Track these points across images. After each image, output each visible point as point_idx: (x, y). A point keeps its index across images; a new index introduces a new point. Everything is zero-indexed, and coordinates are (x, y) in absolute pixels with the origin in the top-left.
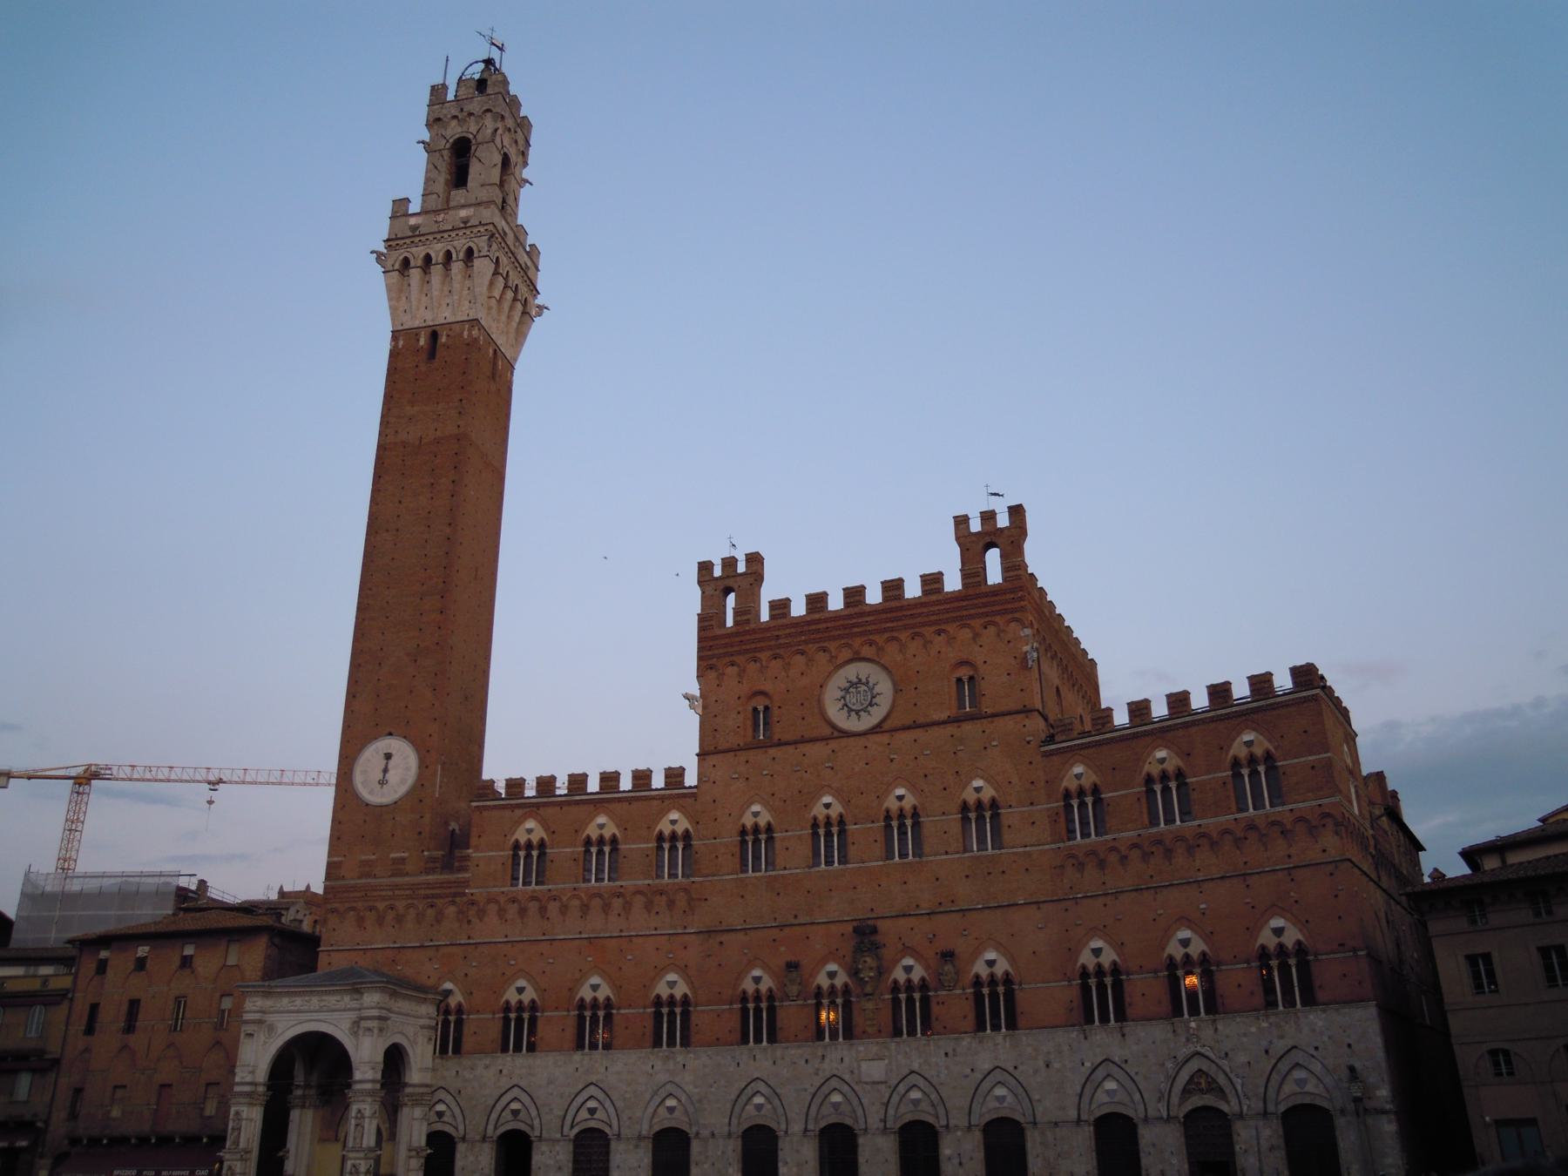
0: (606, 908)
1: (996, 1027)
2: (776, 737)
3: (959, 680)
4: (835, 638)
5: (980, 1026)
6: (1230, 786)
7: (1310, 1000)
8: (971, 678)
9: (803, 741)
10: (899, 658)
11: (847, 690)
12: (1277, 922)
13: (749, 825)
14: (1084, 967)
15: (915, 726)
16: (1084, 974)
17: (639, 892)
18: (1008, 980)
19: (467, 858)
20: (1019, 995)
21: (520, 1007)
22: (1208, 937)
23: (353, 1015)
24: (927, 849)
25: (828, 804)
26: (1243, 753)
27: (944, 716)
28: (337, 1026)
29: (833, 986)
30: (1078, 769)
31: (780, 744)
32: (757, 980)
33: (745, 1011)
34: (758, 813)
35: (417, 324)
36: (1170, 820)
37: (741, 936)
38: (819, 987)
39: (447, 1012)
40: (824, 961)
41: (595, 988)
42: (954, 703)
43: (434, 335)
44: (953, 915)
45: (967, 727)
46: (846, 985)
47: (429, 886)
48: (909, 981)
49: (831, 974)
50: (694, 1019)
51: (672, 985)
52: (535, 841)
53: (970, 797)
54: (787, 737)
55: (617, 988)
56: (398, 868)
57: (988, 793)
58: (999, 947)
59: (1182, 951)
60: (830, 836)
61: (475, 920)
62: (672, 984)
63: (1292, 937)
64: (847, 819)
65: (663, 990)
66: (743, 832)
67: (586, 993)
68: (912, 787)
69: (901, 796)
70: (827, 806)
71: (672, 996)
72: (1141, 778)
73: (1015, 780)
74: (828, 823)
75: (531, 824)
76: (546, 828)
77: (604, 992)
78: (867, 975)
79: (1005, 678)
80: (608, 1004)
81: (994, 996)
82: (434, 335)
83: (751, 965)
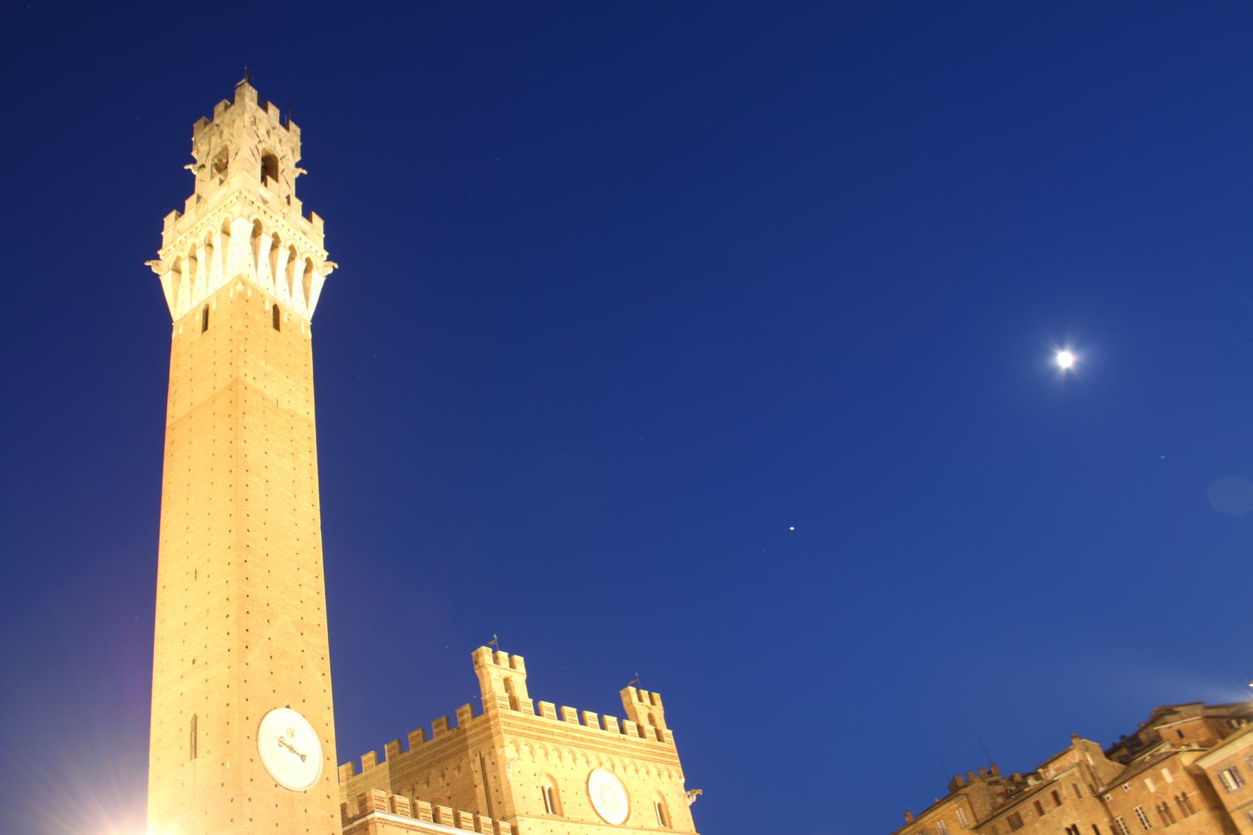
2: (566, 815)
9: (582, 821)
54: (573, 817)
82: (276, 309)
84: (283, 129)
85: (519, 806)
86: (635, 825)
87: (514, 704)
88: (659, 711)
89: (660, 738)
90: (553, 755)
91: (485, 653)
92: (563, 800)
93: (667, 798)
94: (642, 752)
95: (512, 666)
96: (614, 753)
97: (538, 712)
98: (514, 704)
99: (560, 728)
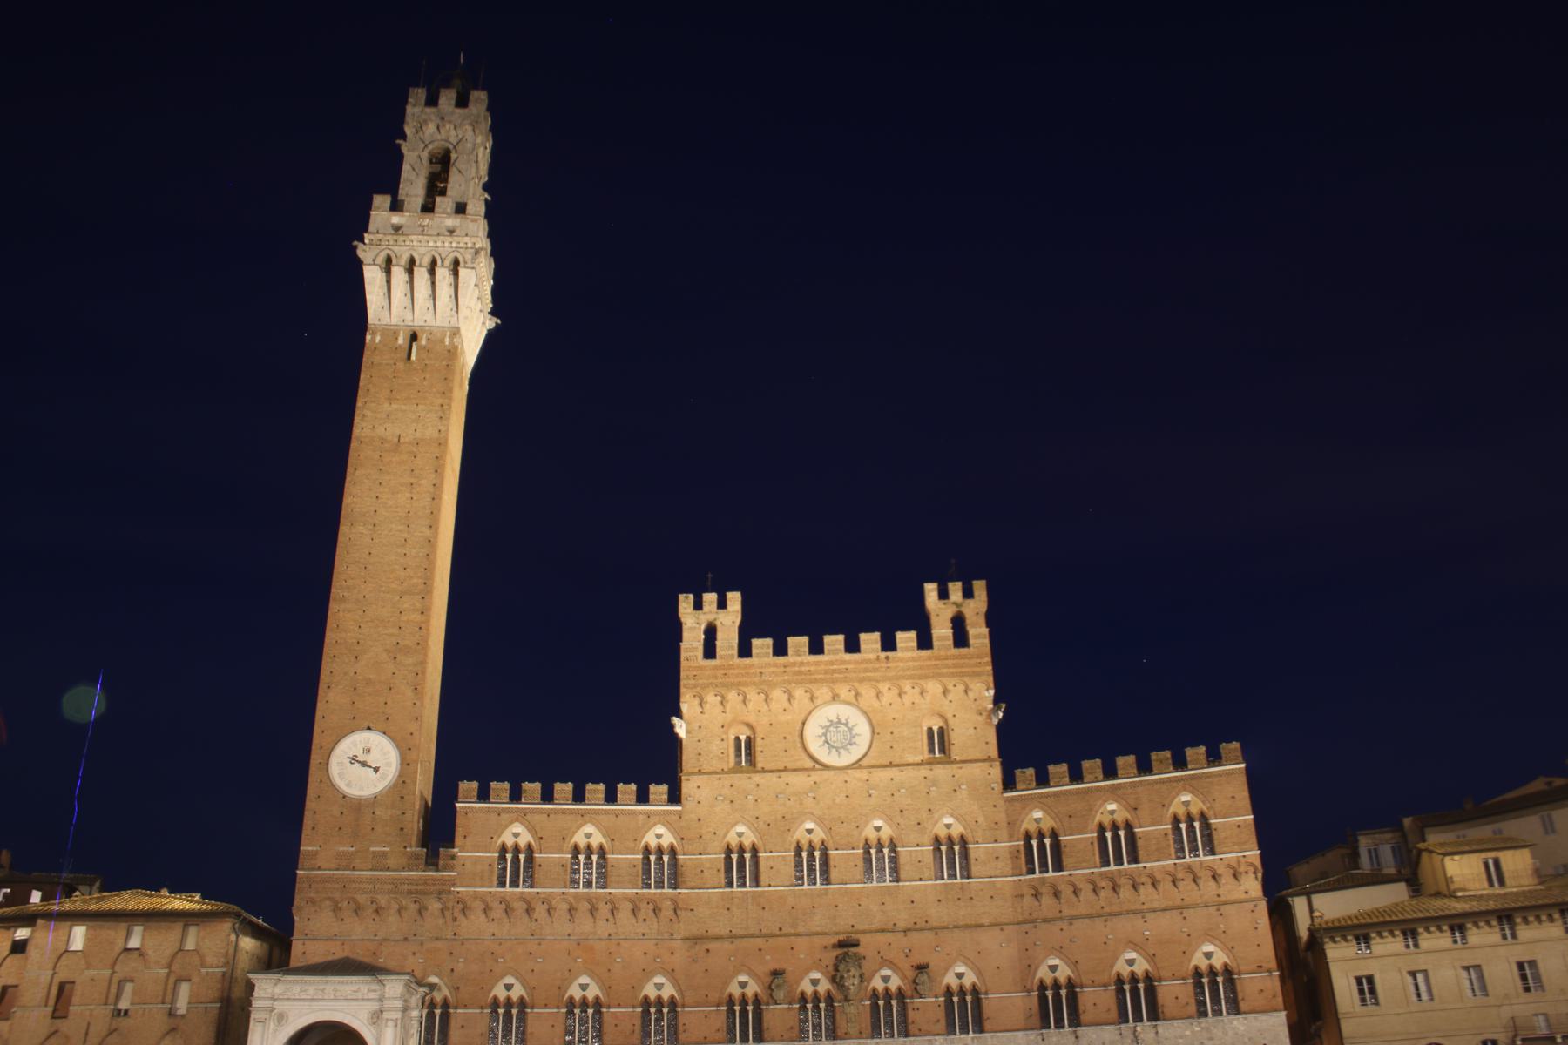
0: (593, 911)
1: (965, 1030)
2: (759, 766)
3: (930, 730)
4: (816, 681)
5: (951, 1029)
6: (1171, 837)
7: (1235, 1008)
8: (941, 731)
9: (785, 770)
10: (876, 704)
11: (827, 728)
12: (1209, 948)
13: (734, 844)
14: (1041, 981)
15: (891, 765)
16: (1042, 987)
17: (626, 898)
18: (975, 991)
19: (453, 857)
20: (985, 1003)
21: (509, 1004)
22: (1151, 958)
23: (375, 1006)
24: (903, 875)
25: (809, 830)
26: (1181, 812)
27: (918, 759)
28: (355, 1017)
29: (816, 993)
30: (1038, 814)
31: (763, 771)
32: (743, 985)
33: (731, 1011)
34: (742, 833)
35: (394, 321)
36: (1119, 861)
37: (726, 945)
38: (803, 993)
39: (432, 1005)
40: (808, 971)
41: (584, 987)
42: (926, 748)
43: (414, 337)
44: (927, 933)
45: (941, 772)
46: (829, 992)
47: (411, 881)
48: (887, 990)
49: (814, 981)
50: (682, 1019)
51: (659, 987)
52: (522, 842)
53: (943, 834)
55: (607, 988)
56: (379, 862)
57: (957, 830)
58: (967, 961)
59: (1129, 969)
60: (814, 863)
61: (461, 917)
62: (659, 986)
63: (1219, 960)
64: (830, 844)
65: (650, 991)
66: (729, 851)
67: (575, 992)
68: (889, 820)
69: (878, 827)
70: (810, 831)
71: (659, 998)
72: (1094, 825)
73: (981, 819)
74: (811, 849)
75: (518, 828)
76: (532, 829)
77: (593, 992)
78: (852, 983)
79: (972, 731)
80: (598, 1004)
81: (963, 1002)
82: (414, 337)
83: (737, 972)
84: (459, 111)
85: (688, 759)
86: (874, 762)
87: (710, 651)
88: (976, 608)
89: (961, 639)
90: (755, 698)
91: (685, 603)
92: (758, 749)
93: (951, 721)
94: (914, 668)
95: (722, 604)
96: (861, 681)
97: (745, 650)
98: (710, 651)
99: (775, 665)
